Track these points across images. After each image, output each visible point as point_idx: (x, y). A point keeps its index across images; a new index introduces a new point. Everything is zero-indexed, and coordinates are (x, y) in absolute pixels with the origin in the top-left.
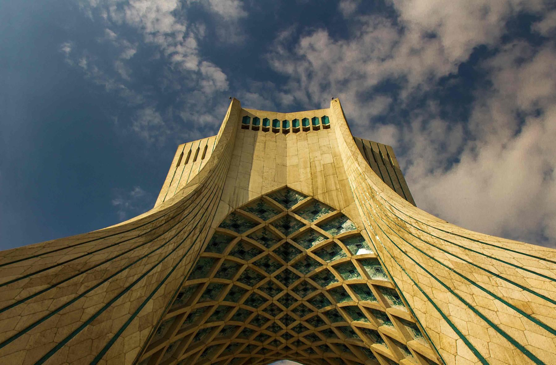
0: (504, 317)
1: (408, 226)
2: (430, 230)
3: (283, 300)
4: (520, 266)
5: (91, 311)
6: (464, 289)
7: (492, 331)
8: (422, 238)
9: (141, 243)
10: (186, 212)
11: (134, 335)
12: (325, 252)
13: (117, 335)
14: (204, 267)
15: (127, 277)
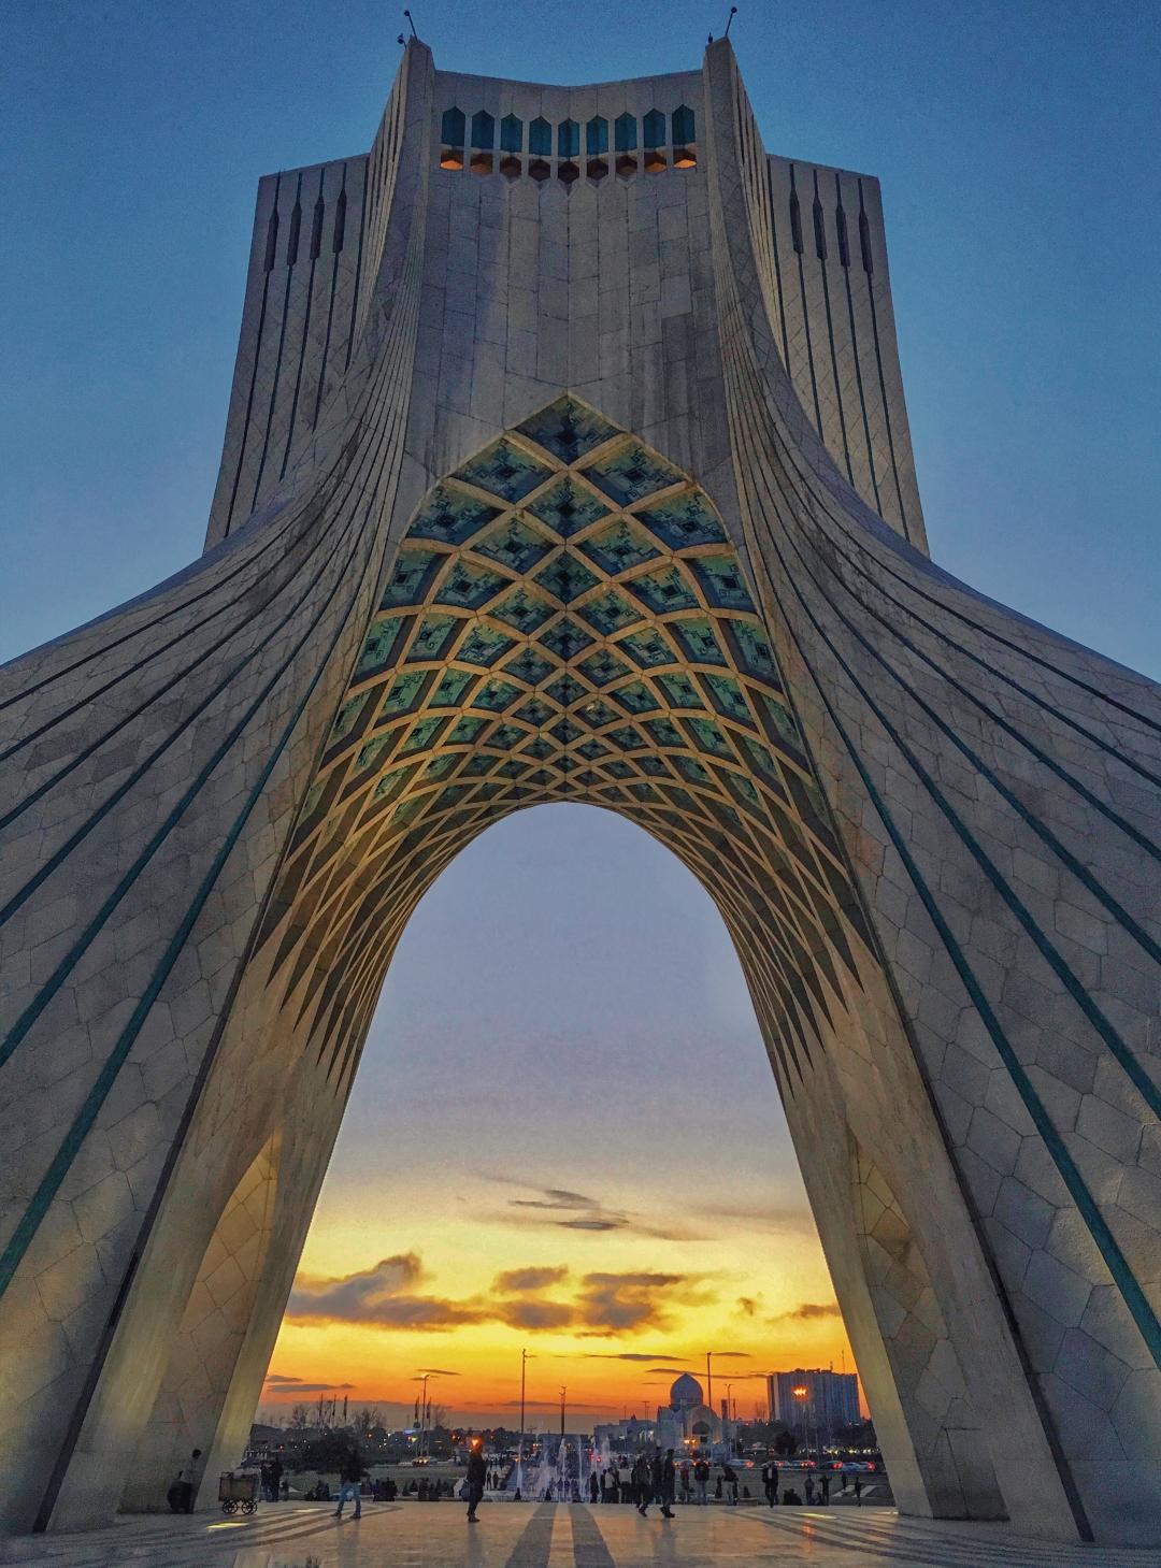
0: (986, 812)
1: (840, 559)
2: (886, 580)
3: (557, 687)
4: (1051, 703)
5: (173, 797)
6: (923, 741)
7: (957, 842)
8: (864, 597)
9: (242, 618)
10: (329, 514)
11: (264, 832)
12: (652, 585)
13: (232, 839)
14: (383, 640)
15: (228, 709)
